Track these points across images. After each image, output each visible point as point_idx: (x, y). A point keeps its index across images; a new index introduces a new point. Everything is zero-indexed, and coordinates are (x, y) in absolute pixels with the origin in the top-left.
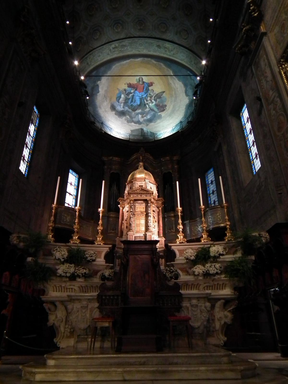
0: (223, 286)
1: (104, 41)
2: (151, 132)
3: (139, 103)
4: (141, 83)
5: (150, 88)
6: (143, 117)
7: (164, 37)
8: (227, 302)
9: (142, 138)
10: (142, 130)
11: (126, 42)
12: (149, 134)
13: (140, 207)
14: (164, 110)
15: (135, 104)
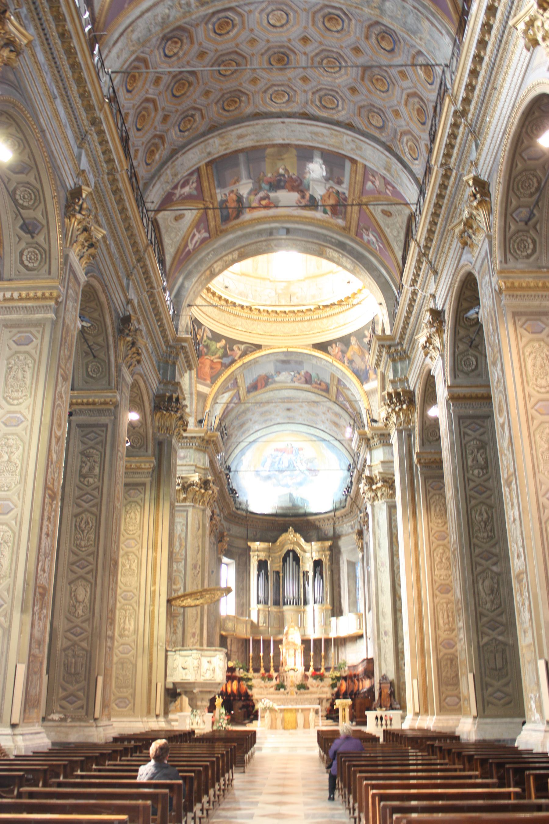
0: (327, 693)
1: (252, 432)
2: (302, 499)
3: (287, 465)
4: (290, 447)
5: (300, 452)
6: (292, 479)
7: (314, 425)
8: (328, 700)
9: (290, 505)
10: (291, 495)
11: (275, 426)
12: (299, 503)
13: (292, 652)
14: (316, 475)
15: (282, 467)
